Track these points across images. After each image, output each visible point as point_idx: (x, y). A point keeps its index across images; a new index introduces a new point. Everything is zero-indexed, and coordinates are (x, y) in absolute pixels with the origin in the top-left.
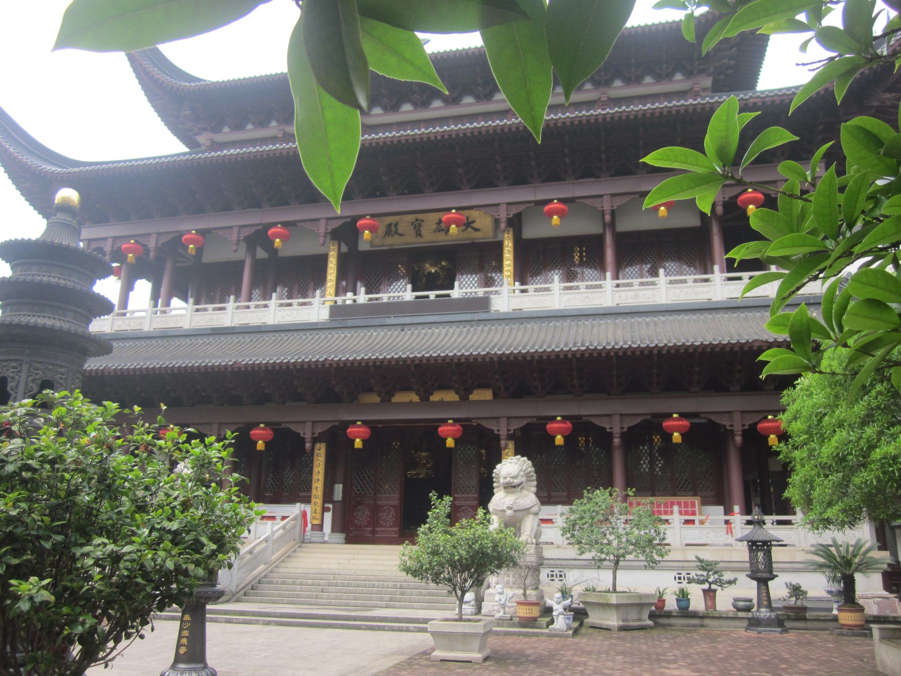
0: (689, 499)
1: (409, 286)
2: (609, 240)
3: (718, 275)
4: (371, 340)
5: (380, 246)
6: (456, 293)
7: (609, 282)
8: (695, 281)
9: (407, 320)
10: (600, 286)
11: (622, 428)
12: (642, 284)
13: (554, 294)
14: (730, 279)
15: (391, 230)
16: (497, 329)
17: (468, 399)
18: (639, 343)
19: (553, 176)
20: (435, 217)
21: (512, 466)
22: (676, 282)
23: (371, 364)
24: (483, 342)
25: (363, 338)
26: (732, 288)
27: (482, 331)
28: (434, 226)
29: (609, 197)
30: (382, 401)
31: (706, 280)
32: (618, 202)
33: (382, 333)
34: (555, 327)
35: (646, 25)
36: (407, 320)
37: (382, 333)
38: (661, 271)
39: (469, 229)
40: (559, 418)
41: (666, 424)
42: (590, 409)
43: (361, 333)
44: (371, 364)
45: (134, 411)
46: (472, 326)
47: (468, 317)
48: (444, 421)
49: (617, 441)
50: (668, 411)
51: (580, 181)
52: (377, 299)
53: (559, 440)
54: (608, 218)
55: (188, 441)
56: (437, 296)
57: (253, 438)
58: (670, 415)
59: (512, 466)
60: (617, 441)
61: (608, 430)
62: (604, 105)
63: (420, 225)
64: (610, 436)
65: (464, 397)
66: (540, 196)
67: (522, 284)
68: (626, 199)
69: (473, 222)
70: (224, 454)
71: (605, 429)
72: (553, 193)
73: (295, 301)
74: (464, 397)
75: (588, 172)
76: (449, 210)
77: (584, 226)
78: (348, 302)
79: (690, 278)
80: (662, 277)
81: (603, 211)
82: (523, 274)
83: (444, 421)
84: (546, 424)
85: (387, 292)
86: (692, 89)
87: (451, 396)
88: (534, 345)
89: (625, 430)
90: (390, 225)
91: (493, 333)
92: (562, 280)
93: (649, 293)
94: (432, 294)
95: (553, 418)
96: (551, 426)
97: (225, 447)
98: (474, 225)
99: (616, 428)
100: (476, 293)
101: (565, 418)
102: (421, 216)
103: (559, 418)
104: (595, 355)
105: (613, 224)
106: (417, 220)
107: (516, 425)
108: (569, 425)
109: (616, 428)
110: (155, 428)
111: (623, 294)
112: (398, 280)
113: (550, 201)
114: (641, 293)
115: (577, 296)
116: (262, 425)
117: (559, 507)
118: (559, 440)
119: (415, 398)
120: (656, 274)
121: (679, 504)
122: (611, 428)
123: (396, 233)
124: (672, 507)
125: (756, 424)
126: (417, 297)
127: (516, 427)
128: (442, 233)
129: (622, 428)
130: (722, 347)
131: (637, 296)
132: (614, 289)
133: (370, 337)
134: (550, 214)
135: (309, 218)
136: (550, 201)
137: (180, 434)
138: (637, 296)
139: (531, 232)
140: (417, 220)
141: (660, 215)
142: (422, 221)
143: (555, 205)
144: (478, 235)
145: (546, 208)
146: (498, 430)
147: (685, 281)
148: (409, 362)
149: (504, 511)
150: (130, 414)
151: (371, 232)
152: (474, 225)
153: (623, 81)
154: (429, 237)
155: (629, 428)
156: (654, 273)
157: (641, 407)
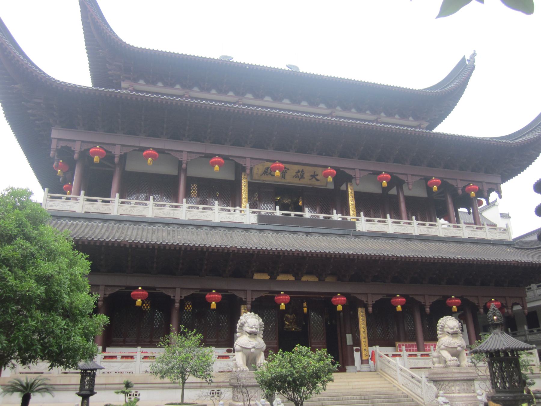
1: (278, 207)
3: (116, 199)
4: (88, 229)
5: (258, 180)
6: (307, 214)
8: (171, 206)
10: (146, 204)
12: (136, 203)
14: (88, 200)
15: (300, 175)
18: (167, 241)
19: (154, 134)
20: (297, 168)
22: (192, 208)
24: (104, 233)
26: (396, 227)
27: (108, 227)
28: (294, 174)
29: (56, 140)
30: (271, 278)
31: (176, 207)
32: (125, 150)
34: (148, 230)
35: (133, 46)
36: (310, 230)
38: (151, 197)
39: (314, 179)
40: (140, 288)
42: (161, 284)
46: (140, 226)
47: (272, 227)
48: (279, 293)
50: (395, 293)
51: (192, 142)
56: (295, 215)
57: (278, 302)
58: (395, 295)
63: (286, 172)
65: (273, 278)
66: (142, 145)
67: (343, 215)
68: (198, 156)
69: (317, 175)
73: (427, 223)
74: (273, 278)
75: (175, 136)
76: (274, 161)
77: (166, 169)
81: (181, 161)
82: (125, 193)
83: (210, 291)
84: (391, 299)
86: (184, 95)
90: (268, 168)
94: (293, 214)
95: (136, 288)
96: (394, 300)
101: (144, 288)
103: (140, 288)
104: (172, 248)
105: (185, 170)
106: (285, 168)
107: (256, 296)
111: (193, 213)
114: (430, 230)
115: (400, 227)
116: (214, 291)
119: (291, 278)
120: (386, 217)
123: (270, 173)
124: (429, 347)
126: (283, 214)
128: (298, 179)
131: (428, 231)
132: (85, 202)
133: (91, 228)
134: (213, 165)
135: (173, 149)
140: (285, 168)
141: (215, 169)
142: (288, 169)
144: (317, 183)
145: (145, 153)
146: (174, 297)
147: (164, 206)
151: (280, 171)
153: (145, 82)
154: (306, 181)
155: (110, 295)
156: (147, 199)
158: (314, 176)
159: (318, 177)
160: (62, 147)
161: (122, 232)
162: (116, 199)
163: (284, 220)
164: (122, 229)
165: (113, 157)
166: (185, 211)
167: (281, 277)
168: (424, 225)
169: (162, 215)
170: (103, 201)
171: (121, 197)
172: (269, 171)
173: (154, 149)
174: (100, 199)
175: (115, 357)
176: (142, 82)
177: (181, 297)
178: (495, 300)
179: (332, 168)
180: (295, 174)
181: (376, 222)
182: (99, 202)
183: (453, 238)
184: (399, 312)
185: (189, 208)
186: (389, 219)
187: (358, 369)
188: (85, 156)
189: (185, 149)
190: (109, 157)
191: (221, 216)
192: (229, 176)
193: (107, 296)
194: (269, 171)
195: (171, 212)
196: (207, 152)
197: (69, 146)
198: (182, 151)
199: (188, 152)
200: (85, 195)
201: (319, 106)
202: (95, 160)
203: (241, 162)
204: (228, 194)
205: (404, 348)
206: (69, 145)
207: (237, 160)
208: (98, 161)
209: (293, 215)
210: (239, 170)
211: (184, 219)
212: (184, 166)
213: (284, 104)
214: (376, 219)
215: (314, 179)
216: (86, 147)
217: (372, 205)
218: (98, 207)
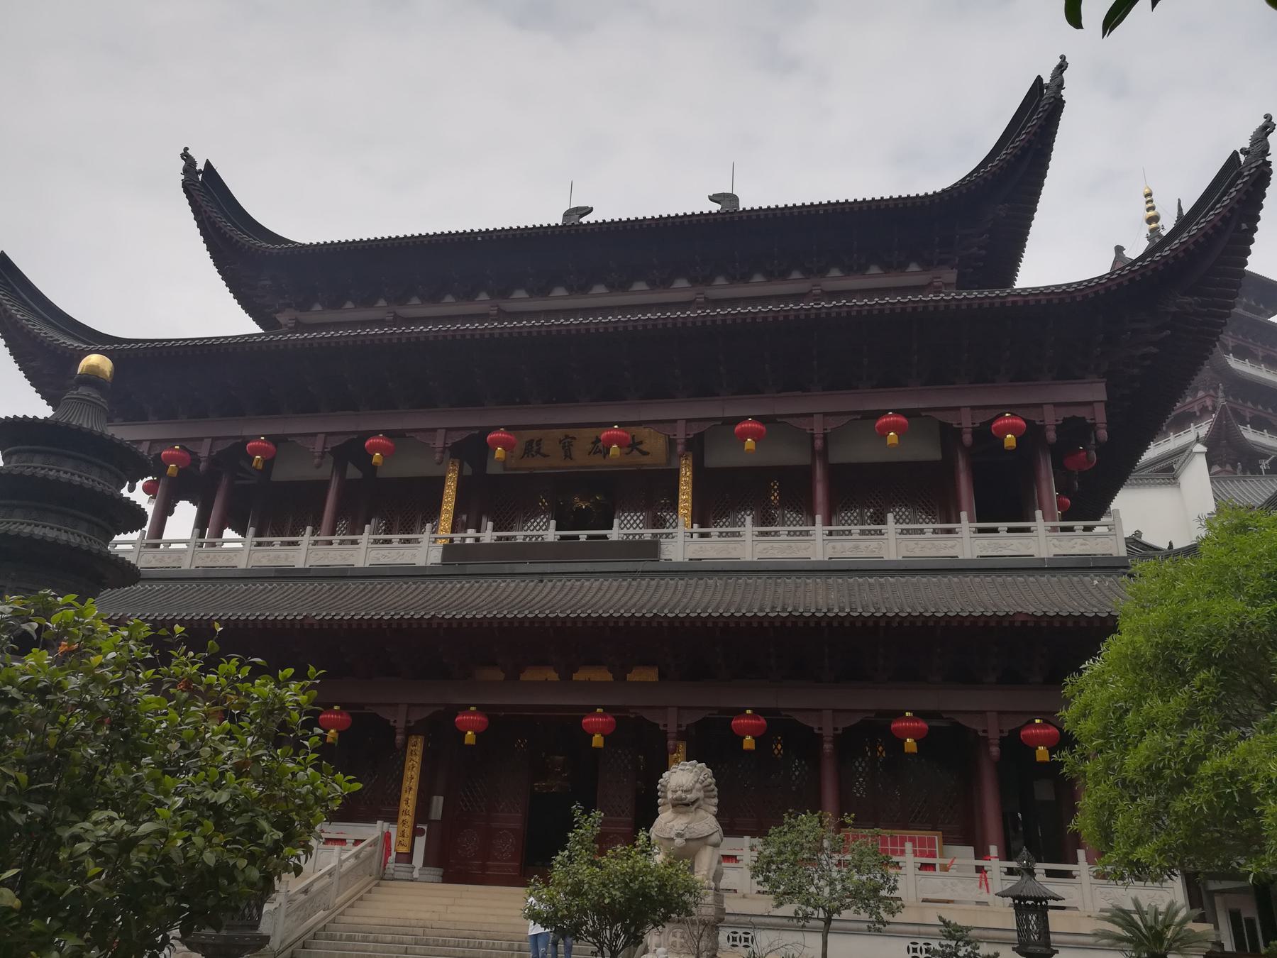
0: (926, 835)
1: (553, 523)
2: (819, 473)
3: (966, 525)
6: (615, 534)
8: (935, 531)
9: (548, 568)
10: (807, 533)
11: (836, 729)
12: (862, 532)
13: (746, 543)
14: (981, 531)
15: (532, 448)
20: (590, 433)
21: (683, 776)
22: (908, 531)
25: (487, 589)
26: (985, 542)
27: (648, 585)
31: (949, 531)
33: (513, 585)
36: (548, 568)
37: (513, 585)
38: (890, 517)
39: (635, 452)
40: (749, 712)
42: (792, 700)
45: (173, 632)
51: (783, 394)
52: (507, 538)
54: (819, 443)
55: (251, 679)
56: (589, 537)
59: (683, 776)
60: (827, 747)
64: (818, 739)
66: (729, 413)
68: (846, 419)
69: (641, 443)
70: (302, 698)
71: (812, 729)
72: (747, 409)
77: (789, 455)
78: (468, 541)
79: (929, 527)
80: (891, 525)
82: (702, 516)
83: (591, 710)
88: (718, 607)
89: (840, 732)
90: (530, 443)
91: (662, 589)
92: (755, 523)
93: (874, 544)
94: (583, 535)
95: (740, 712)
97: (304, 690)
98: (641, 447)
99: (828, 728)
102: (571, 432)
105: (824, 453)
106: (567, 437)
107: (689, 719)
108: (762, 721)
109: (828, 728)
110: (205, 659)
111: (838, 545)
112: (536, 516)
113: (744, 419)
114: (862, 545)
115: (775, 545)
117: (747, 838)
119: (553, 676)
120: (883, 521)
121: (912, 840)
122: (820, 729)
123: (538, 452)
126: (562, 538)
127: (689, 722)
129: (836, 729)
131: (857, 548)
134: (743, 436)
137: (238, 668)
139: (718, 458)
143: (749, 425)
144: (645, 460)
145: (738, 428)
146: (665, 725)
147: (922, 531)
149: (673, 839)
150: (168, 636)
151: (504, 448)
152: (641, 447)
154: (582, 459)
155: (844, 729)
158: (633, 445)
159: (644, 447)
162: (966, 525)
163: (564, 550)
164: (666, 588)
165: (959, 432)
166: (817, 543)
167: (529, 675)
168: (388, 542)
170: (1010, 530)
171: (257, 534)
172: (535, 448)
174: (1003, 526)
175: (343, 841)
176: (720, 281)
178: (1045, 721)
179: (897, 412)
180: (591, 446)
182: (1003, 533)
184: (749, 751)
185: (902, 533)
186: (749, 528)
187: (416, 874)
188: (986, 436)
189: (815, 408)
190: (1031, 436)
191: (761, 546)
192: (928, 451)
194: (535, 448)
195: (283, 554)
196: (726, 415)
199: (973, 408)
201: (675, 286)
202: (1006, 445)
203: (949, 418)
204: (405, 507)
205: (908, 846)
207: (940, 416)
208: (1014, 444)
209: (583, 538)
210: (949, 436)
211: (820, 558)
212: (819, 443)
213: (872, 276)
215: (635, 452)
216: (981, 418)
218: (1005, 543)
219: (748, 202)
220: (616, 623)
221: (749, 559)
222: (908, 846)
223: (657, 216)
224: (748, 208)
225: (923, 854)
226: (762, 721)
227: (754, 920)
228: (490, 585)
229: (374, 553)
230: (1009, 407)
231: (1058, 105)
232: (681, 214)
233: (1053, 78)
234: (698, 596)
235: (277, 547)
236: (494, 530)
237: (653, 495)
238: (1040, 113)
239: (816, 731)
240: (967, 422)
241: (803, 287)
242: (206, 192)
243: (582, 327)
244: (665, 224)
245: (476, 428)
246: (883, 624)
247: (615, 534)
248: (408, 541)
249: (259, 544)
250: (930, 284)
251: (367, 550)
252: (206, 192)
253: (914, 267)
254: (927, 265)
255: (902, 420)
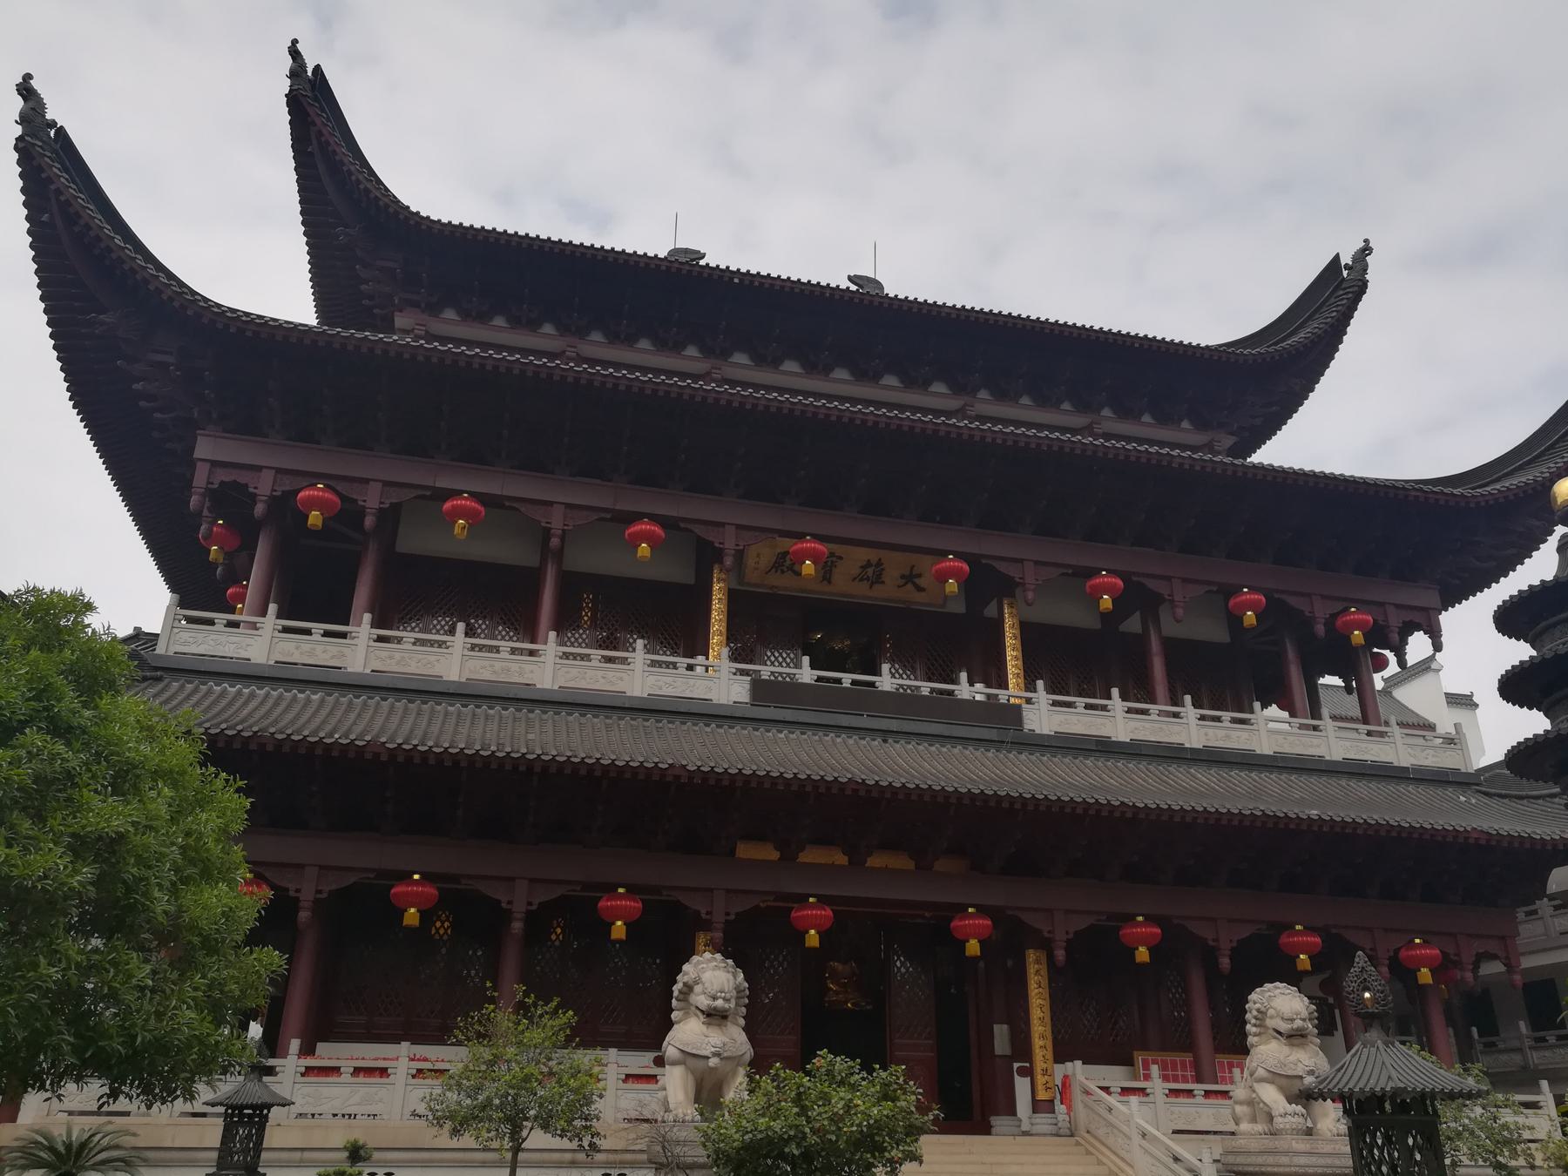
0: (1178, 1058)
1: (806, 660)
3: (363, 629)
4: (279, 709)
5: (756, 585)
6: (886, 681)
7: (551, 647)
8: (513, 651)
9: (894, 725)
10: (441, 644)
11: (320, 892)
13: (453, 656)
14: (286, 630)
16: (433, 711)
17: (732, 852)
19: (474, 456)
21: (711, 975)
23: (739, 784)
26: (1138, 724)
28: (856, 571)
31: (532, 653)
32: (394, 497)
34: (447, 714)
36: (894, 725)
38: (461, 626)
39: (910, 586)
40: (416, 877)
41: (399, 889)
43: (810, 737)
44: (739, 784)
46: (425, 703)
47: (788, 715)
49: (517, 926)
53: (412, 915)
56: (854, 682)
58: (1133, 917)
59: (711, 975)
60: (517, 926)
61: (292, 893)
62: (721, 382)
65: (788, 857)
66: (443, 483)
67: (988, 686)
69: (919, 576)
71: (499, 902)
73: (1226, 715)
74: (788, 857)
76: (800, 536)
78: (979, 697)
79: (505, 645)
80: (639, 654)
82: (391, 614)
83: (610, 889)
85: (413, 630)
87: (902, 862)
88: (331, 735)
91: (453, 721)
93: (1245, 735)
94: (847, 679)
96: (1128, 932)
98: (917, 581)
99: (519, 901)
100: (918, 688)
102: (838, 549)
103: (416, 877)
105: (559, 554)
106: (832, 554)
108: (828, 912)
109: (519, 901)
111: (574, 672)
113: (457, 493)
114: (1234, 734)
115: (1147, 725)
116: (621, 890)
118: (412, 915)
119: (841, 859)
121: (1155, 1062)
122: (509, 903)
123: (791, 568)
125: (1397, 951)
126: (819, 679)
128: (866, 584)
130: (748, 779)
132: (277, 634)
133: (289, 707)
136: (458, 493)
138: (1228, 736)
139: (414, 540)
140: (832, 554)
143: (464, 502)
145: (448, 505)
147: (497, 650)
148: (598, 773)
152: (917, 581)
154: (889, 591)
157: (359, 856)
158: (910, 578)
159: (921, 582)
160: (222, 483)
161: (372, 718)
162: (363, 629)
164: (376, 711)
165: (361, 513)
166: (550, 666)
167: (810, 856)
168: (1218, 719)
169: (486, 675)
170: (327, 634)
171: (376, 624)
172: (788, 563)
173: (473, 495)
174: (318, 627)
175: (335, 1070)
177: (530, 904)
179: (958, 555)
181: (1081, 710)
182: (316, 637)
183: (1300, 759)
184: (1143, 964)
186: (1116, 702)
187: (1025, 1127)
188: (285, 509)
189: (559, 497)
190: (347, 515)
192: (678, 572)
193: (325, 895)
194: (788, 563)
195: (514, 667)
197: (242, 480)
198: (551, 503)
199: (569, 506)
200: (278, 617)
202: (311, 521)
205: (1155, 1069)
206: (243, 477)
207: (699, 530)
208: (320, 523)
209: (846, 683)
211: (547, 686)
212: (555, 542)
214: (1081, 701)
215: (910, 586)
216: (287, 484)
217: (1070, 663)
218: (313, 648)
219: (897, 286)
220: (828, 789)
221: (637, 693)
222: (1155, 1069)
223: (723, 267)
224: (892, 295)
225: (1176, 1080)
226: (828, 912)
227: (307, 1155)
228: (182, 687)
229: (471, 664)
230: (320, 477)
231: (1362, 287)
232: (1005, 312)
233: (1355, 259)
234: (379, 721)
235: (595, 663)
236: (278, 617)
237: (958, 643)
238: (1336, 294)
239: (504, 905)
240: (264, 486)
241: (700, 367)
242: (312, 107)
243: (965, 431)
244: (530, 246)
245: (1069, 566)
246: (319, 751)
247: (886, 681)
248: (609, 660)
249: (380, 639)
250: (708, 373)
251: (639, 674)
252: (312, 107)
253: (692, 351)
254: (1201, 424)
255: (657, 529)
